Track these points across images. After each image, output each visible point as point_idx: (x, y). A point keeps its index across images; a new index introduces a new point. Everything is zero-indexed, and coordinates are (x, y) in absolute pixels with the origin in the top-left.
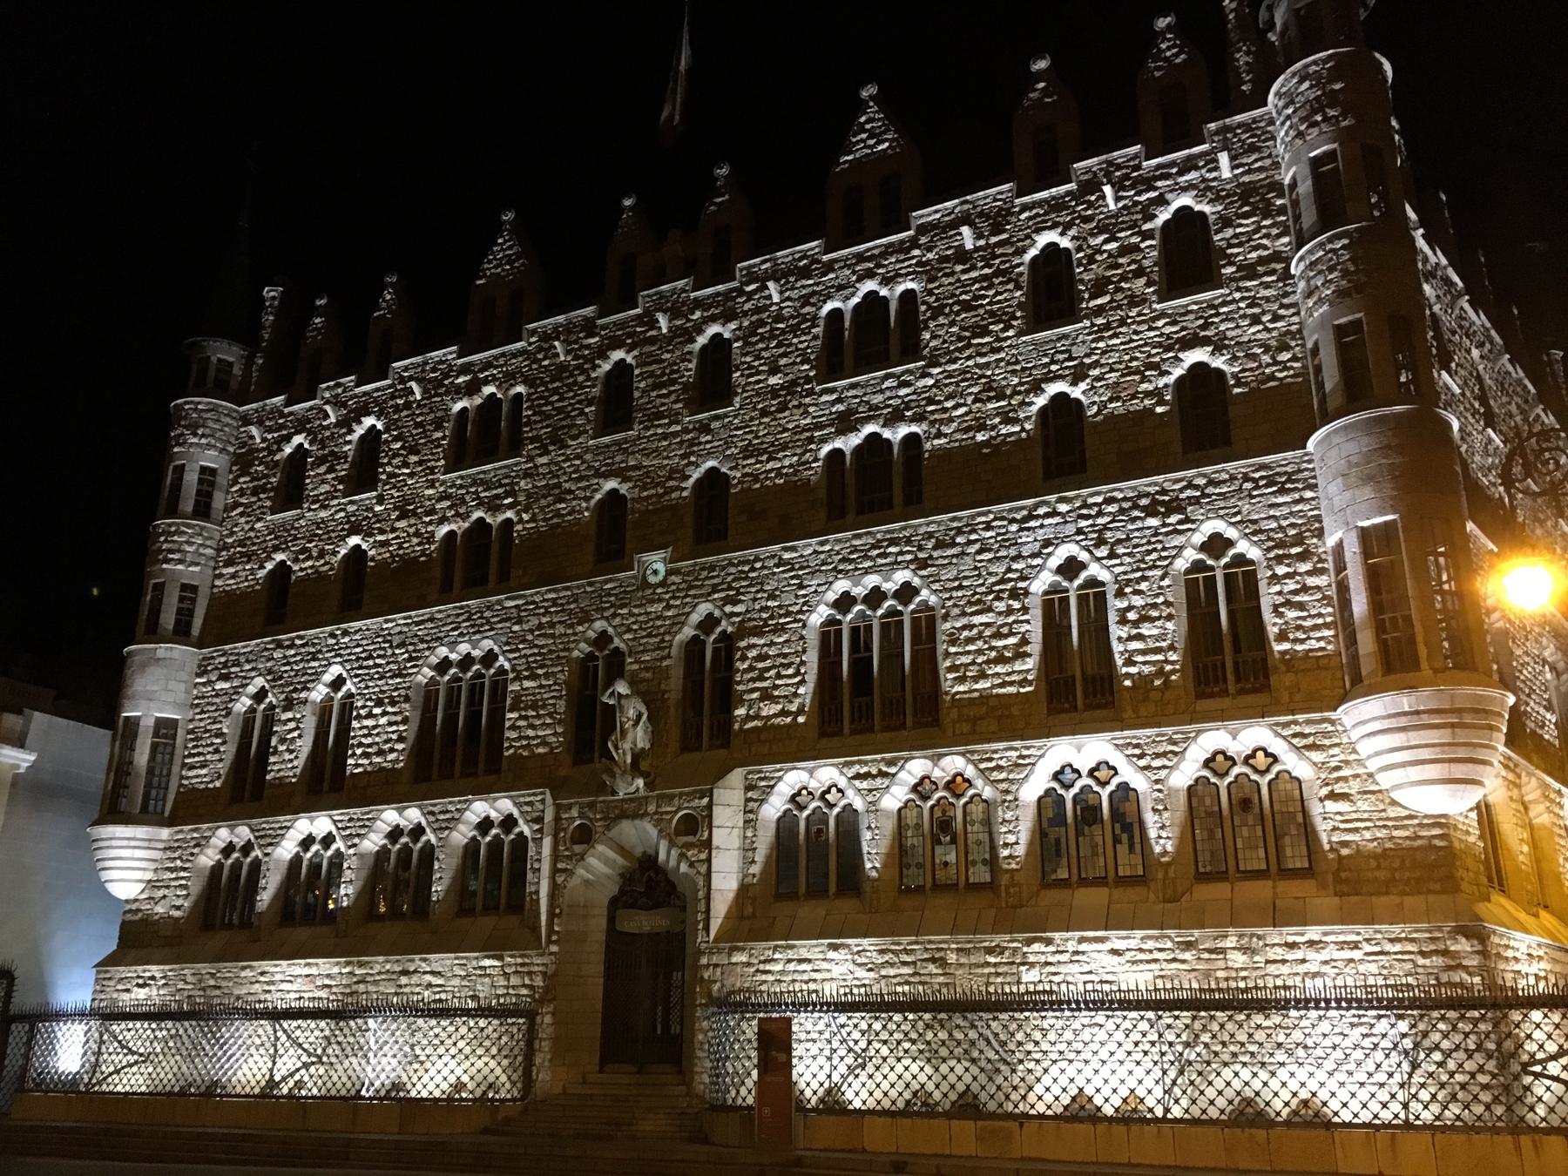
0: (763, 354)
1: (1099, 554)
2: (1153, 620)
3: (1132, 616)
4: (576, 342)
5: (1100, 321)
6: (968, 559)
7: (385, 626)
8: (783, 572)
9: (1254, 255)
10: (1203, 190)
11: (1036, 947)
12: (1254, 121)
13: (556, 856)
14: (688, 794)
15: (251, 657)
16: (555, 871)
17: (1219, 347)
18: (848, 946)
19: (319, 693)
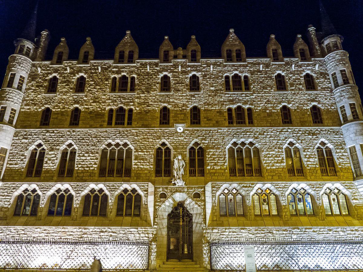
0: (209, 82)
1: (299, 142)
2: (312, 158)
3: (307, 156)
4: (152, 67)
5: (293, 92)
6: (268, 139)
7: (89, 131)
8: (219, 135)
9: (324, 86)
10: (312, 71)
11: (295, 230)
12: (321, 60)
13: (155, 201)
14: (197, 187)
15: (36, 134)
16: (155, 205)
17: (319, 102)
18: (246, 229)
19: (63, 147)
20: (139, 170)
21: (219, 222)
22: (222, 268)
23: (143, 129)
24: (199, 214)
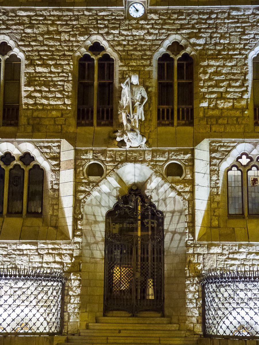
8: (232, 23)
13: (77, 183)
14: (174, 151)
16: (76, 192)
20: (37, 109)
21: (223, 231)
22: (228, 333)
23: (45, 10)
24: (178, 211)
